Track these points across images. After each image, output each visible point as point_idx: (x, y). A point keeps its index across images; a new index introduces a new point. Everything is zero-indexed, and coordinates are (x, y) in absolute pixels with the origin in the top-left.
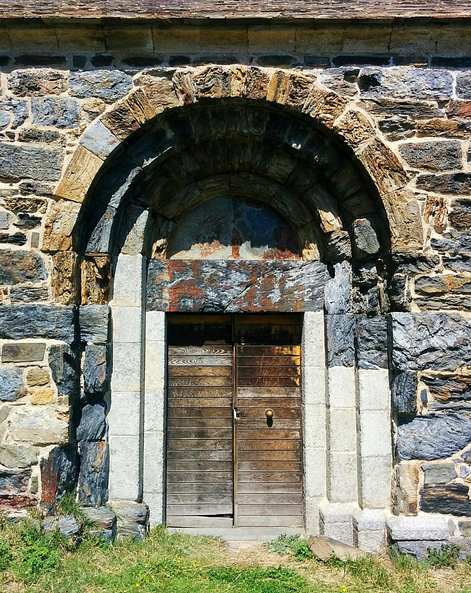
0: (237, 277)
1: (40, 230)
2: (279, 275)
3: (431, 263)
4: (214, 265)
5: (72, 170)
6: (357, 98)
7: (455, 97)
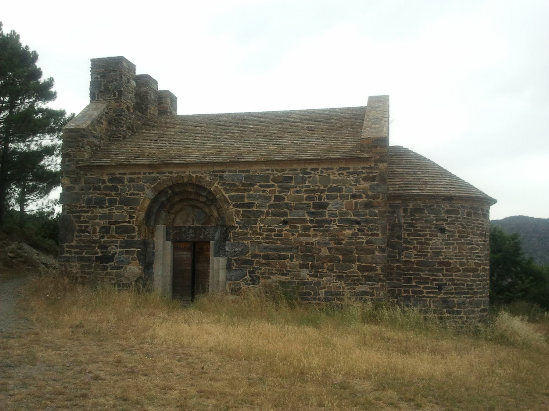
0: (191, 231)
1: (134, 220)
2: (203, 230)
3: (236, 228)
4: (185, 227)
5: (143, 203)
6: (217, 182)
7: (243, 181)
